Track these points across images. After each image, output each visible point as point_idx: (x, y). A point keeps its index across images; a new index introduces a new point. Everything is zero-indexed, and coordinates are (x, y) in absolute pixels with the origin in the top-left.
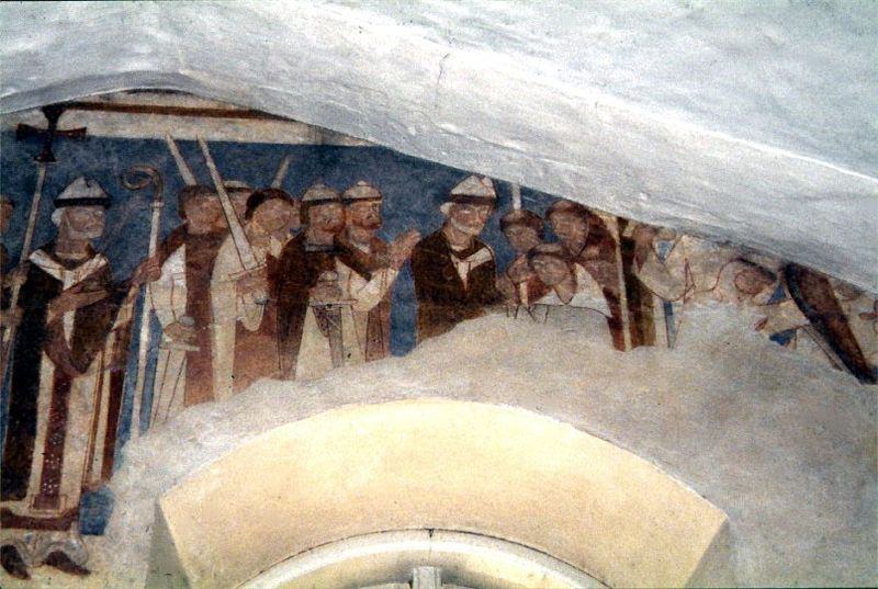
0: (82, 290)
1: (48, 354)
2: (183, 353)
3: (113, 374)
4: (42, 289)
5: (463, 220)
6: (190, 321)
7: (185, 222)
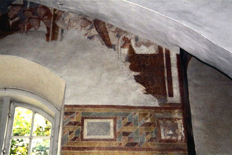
5: (13, 10)
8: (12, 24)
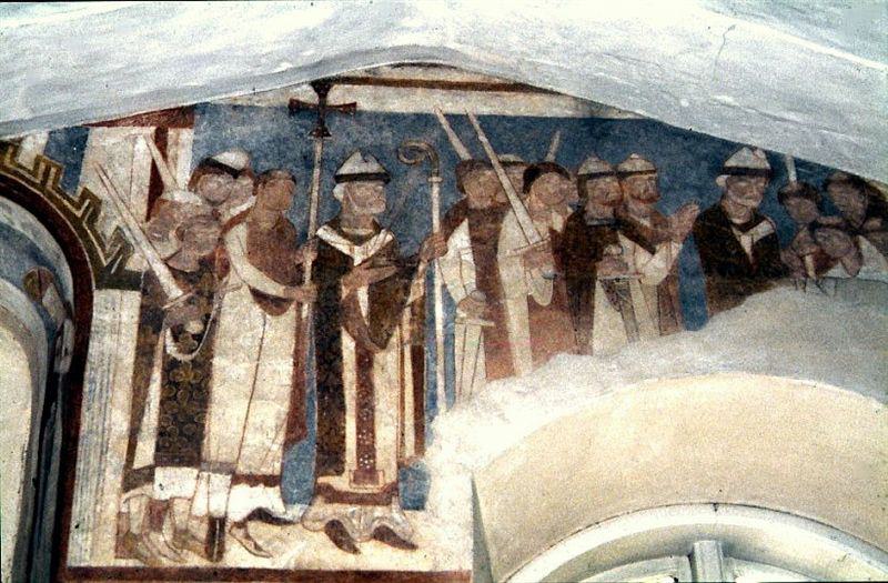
0: (372, 266)
1: (347, 329)
2: (479, 328)
4: (332, 265)
5: (742, 193)
6: (479, 295)
7: (465, 196)
8: (753, 247)
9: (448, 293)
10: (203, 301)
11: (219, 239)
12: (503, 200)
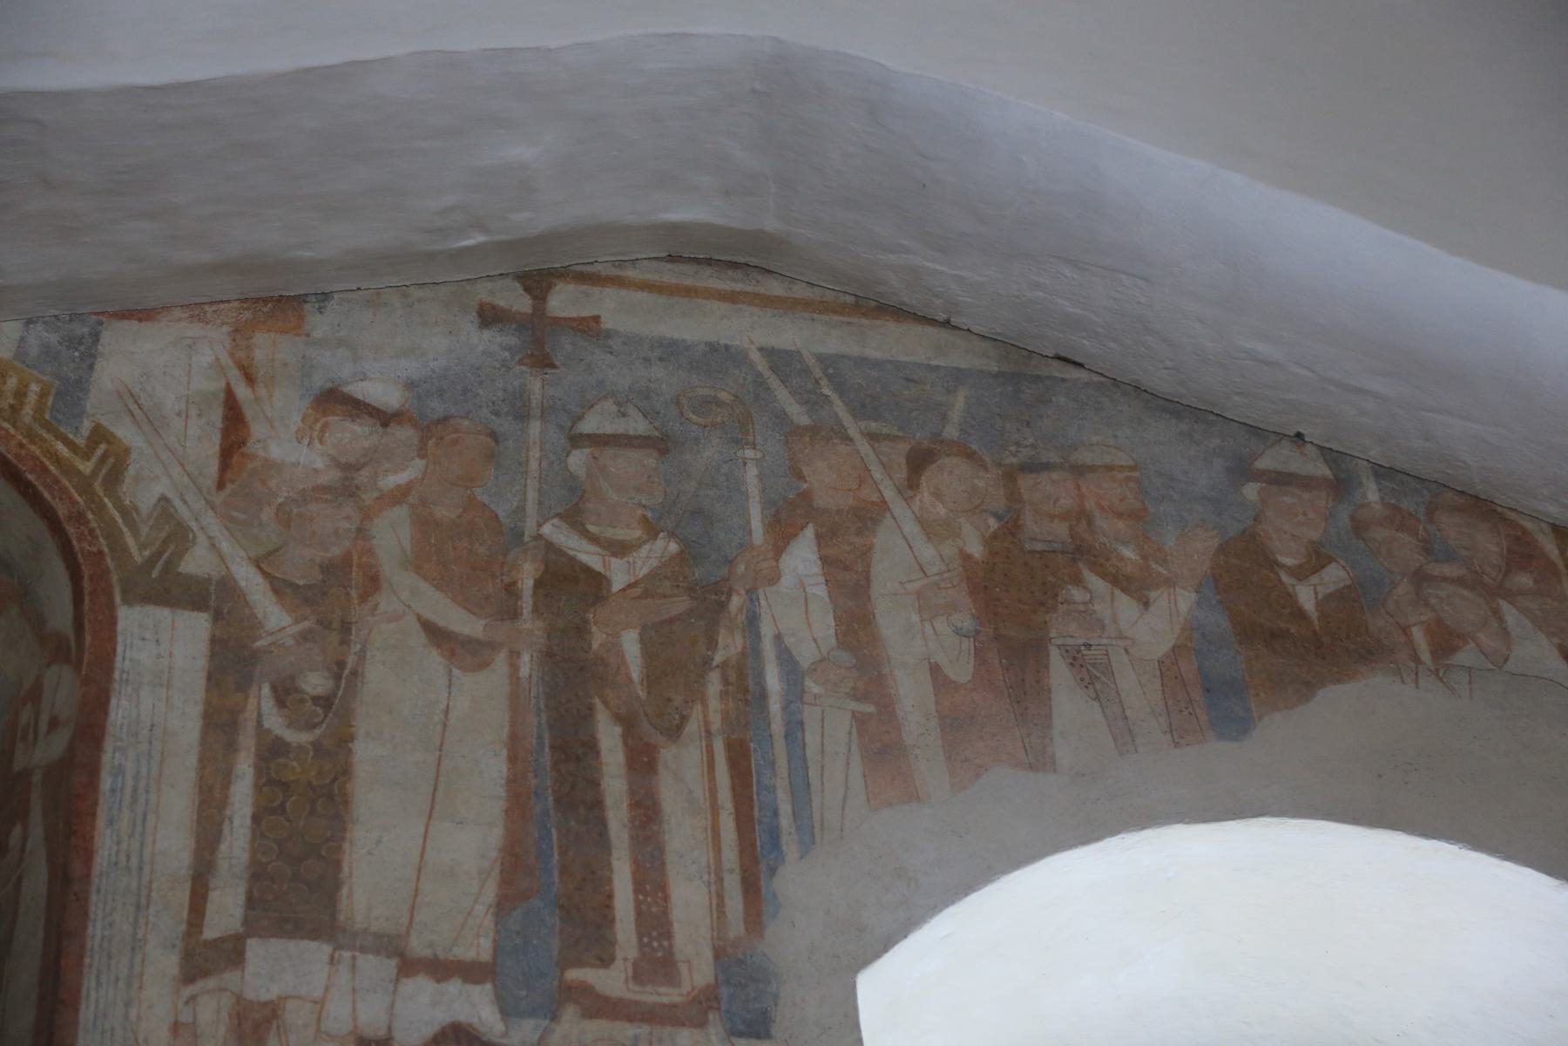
0: (646, 594)
1: (605, 703)
3: (729, 746)
6: (846, 658)
7: (805, 486)
8: (1318, 604)
9: (787, 650)
10: (334, 638)
11: (359, 530)
12: (875, 497)
